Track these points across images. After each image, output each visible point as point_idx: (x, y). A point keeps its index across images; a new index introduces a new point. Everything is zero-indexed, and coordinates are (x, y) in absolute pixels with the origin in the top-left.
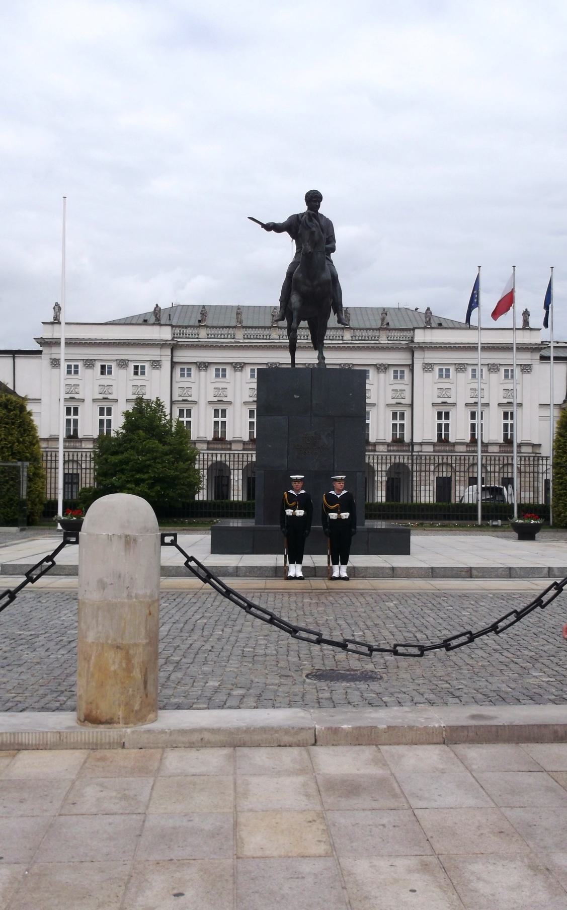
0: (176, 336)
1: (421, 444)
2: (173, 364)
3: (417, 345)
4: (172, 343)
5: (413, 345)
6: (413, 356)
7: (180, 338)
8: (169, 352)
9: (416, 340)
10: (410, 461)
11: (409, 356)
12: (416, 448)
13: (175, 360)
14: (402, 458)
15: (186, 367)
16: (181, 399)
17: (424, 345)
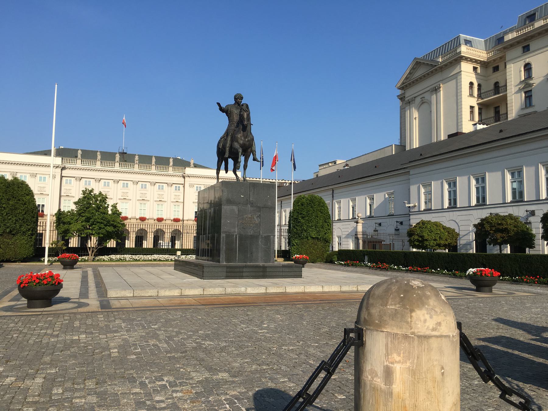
0: (64, 163)
1: (187, 220)
2: (62, 177)
3: (187, 175)
4: (62, 166)
5: (184, 175)
6: (184, 180)
7: (66, 164)
8: (59, 170)
9: (186, 173)
10: (182, 228)
11: (183, 179)
12: (185, 222)
13: (62, 175)
14: (178, 226)
15: (69, 179)
16: (65, 195)
17: (190, 175)
